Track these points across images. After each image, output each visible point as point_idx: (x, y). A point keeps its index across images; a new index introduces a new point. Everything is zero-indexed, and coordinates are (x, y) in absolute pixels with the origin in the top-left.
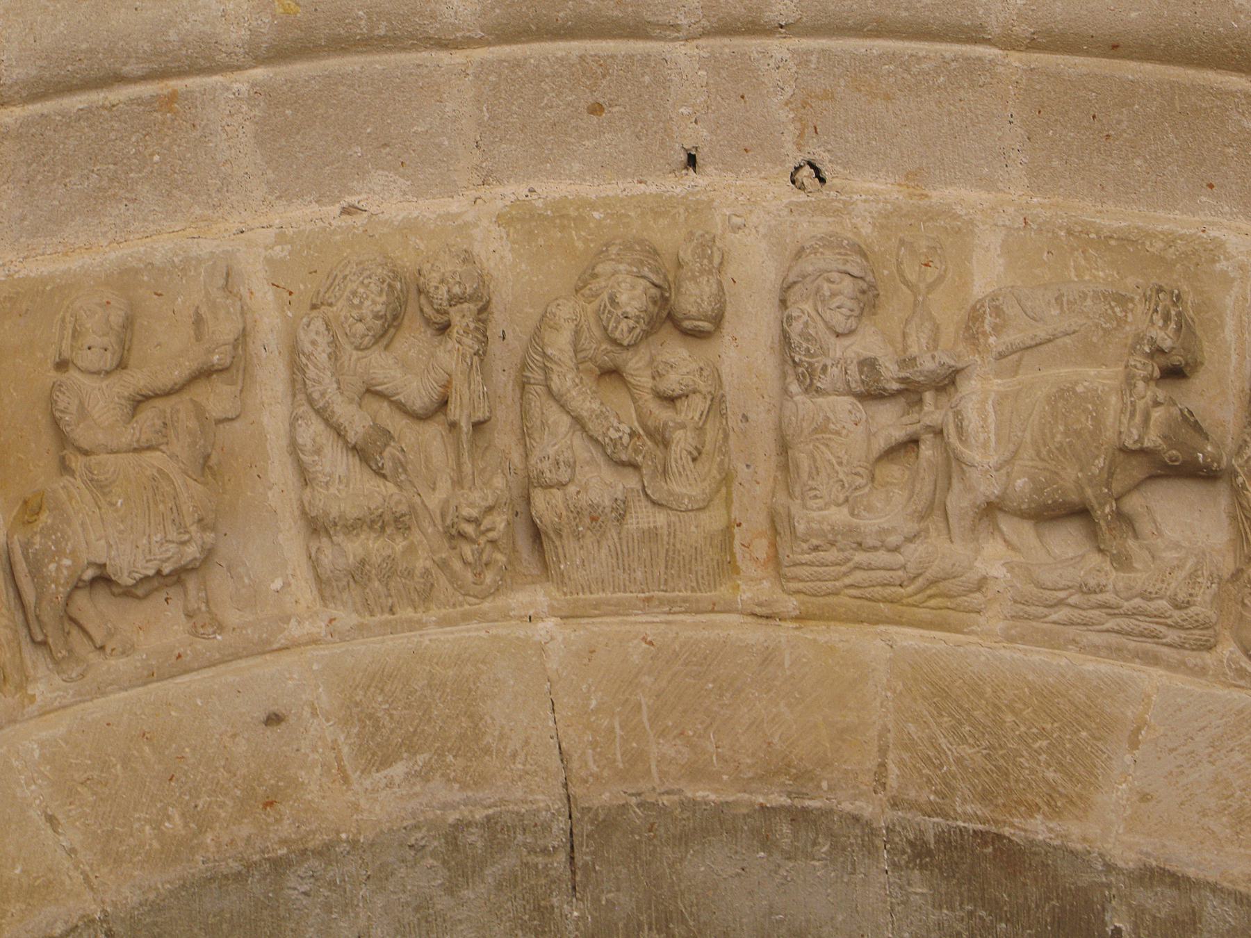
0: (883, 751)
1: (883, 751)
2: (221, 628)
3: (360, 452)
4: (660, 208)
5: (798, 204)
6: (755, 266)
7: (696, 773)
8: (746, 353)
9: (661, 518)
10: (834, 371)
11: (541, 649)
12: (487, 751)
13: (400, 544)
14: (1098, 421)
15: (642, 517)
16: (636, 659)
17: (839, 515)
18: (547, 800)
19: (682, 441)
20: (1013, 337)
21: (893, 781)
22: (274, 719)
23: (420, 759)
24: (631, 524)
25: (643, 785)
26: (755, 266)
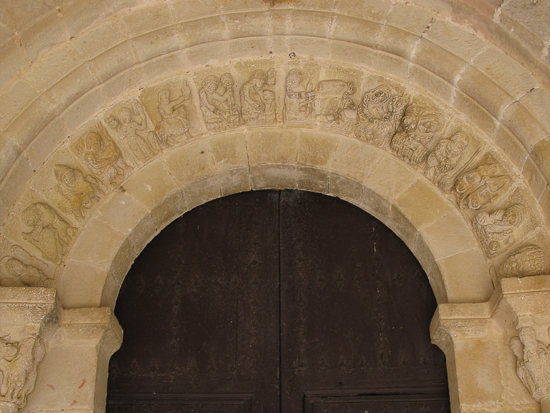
0: (297, 154)
1: (297, 154)
2: (192, 137)
3: (214, 112)
4: (265, 62)
5: (290, 62)
6: (281, 72)
7: (268, 160)
8: (279, 88)
9: (264, 117)
10: (294, 96)
11: (245, 135)
12: (236, 157)
13: (221, 124)
14: (337, 105)
15: (261, 117)
16: (260, 137)
17: (294, 116)
18: (246, 166)
19: (268, 106)
20: (324, 91)
21: (298, 159)
22: (202, 153)
23: (226, 159)
24: (259, 118)
25: (260, 162)
26: (281, 72)
